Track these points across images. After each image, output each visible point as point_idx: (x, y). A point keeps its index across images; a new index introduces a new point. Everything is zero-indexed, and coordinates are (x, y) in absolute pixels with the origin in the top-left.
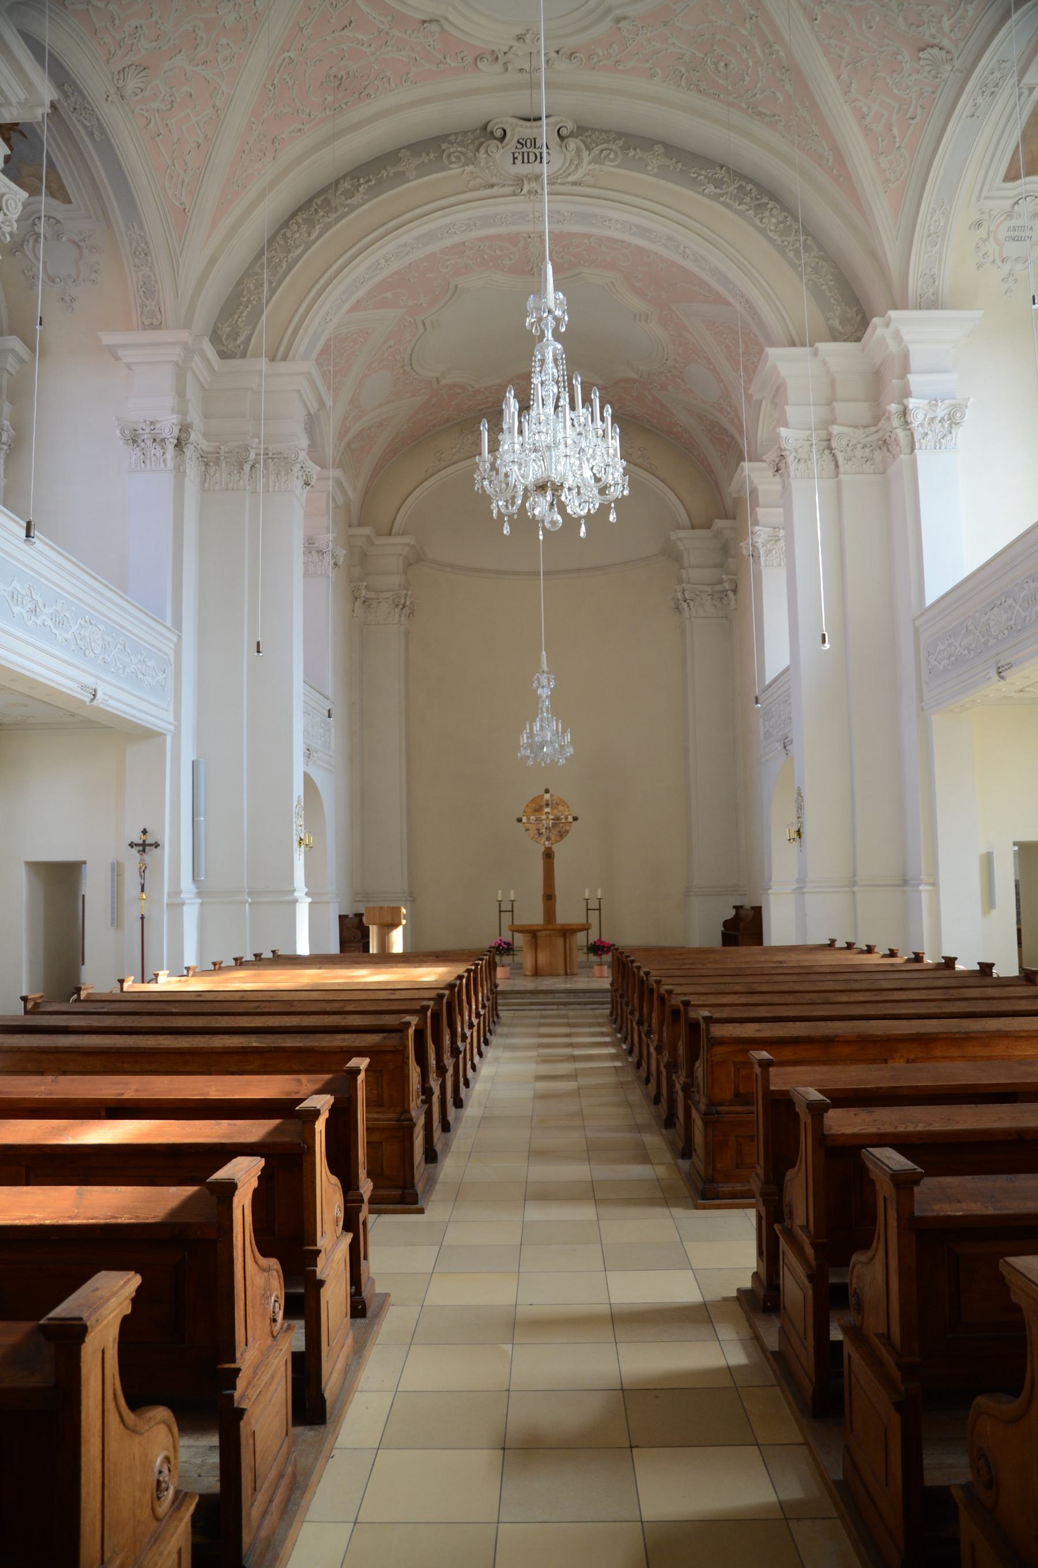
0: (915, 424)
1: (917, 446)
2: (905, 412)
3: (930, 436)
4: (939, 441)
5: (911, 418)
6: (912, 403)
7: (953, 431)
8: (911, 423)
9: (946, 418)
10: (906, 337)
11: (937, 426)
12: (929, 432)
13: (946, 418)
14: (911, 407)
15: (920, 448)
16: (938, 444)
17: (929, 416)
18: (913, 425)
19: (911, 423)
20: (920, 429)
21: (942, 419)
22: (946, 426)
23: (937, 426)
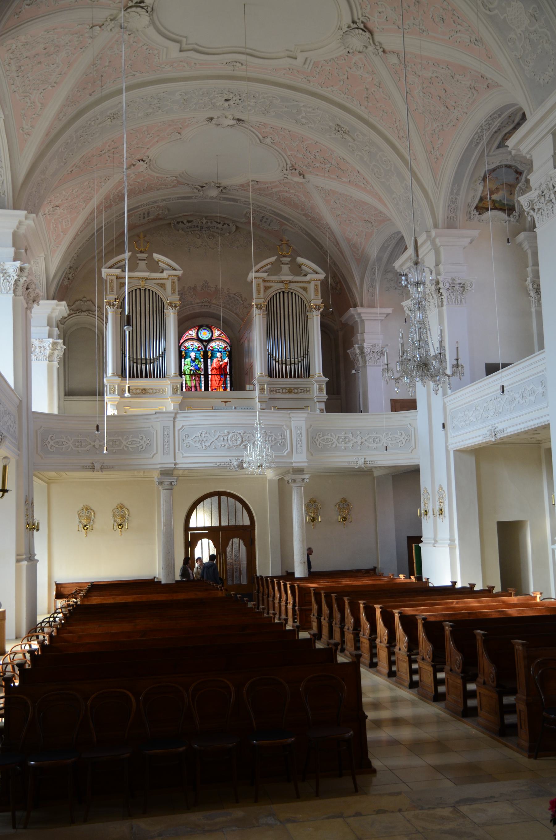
0: (367, 354)
1: (367, 362)
2: (362, 348)
3: (373, 359)
4: (376, 361)
5: (365, 350)
6: (366, 345)
7: (382, 357)
8: (365, 353)
9: (379, 352)
10: (363, 318)
11: (375, 354)
12: (372, 357)
13: (379, 352)
14: (365, 347)
15: (369, 364)
16: (376, 362)
17: (372, 350)
18: (366, 354)
19: (365, 353)
20: (369, 355)
21: (378, 352)
22: (379, 355)
23: (375, 354)
